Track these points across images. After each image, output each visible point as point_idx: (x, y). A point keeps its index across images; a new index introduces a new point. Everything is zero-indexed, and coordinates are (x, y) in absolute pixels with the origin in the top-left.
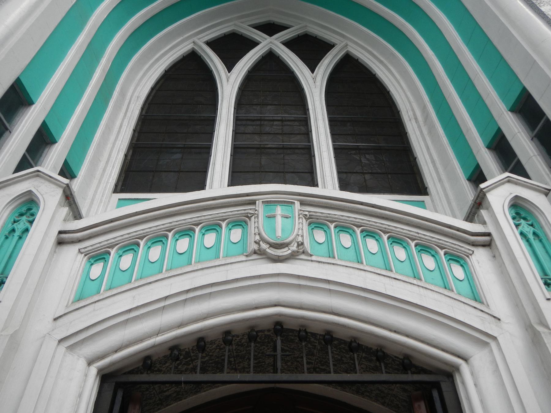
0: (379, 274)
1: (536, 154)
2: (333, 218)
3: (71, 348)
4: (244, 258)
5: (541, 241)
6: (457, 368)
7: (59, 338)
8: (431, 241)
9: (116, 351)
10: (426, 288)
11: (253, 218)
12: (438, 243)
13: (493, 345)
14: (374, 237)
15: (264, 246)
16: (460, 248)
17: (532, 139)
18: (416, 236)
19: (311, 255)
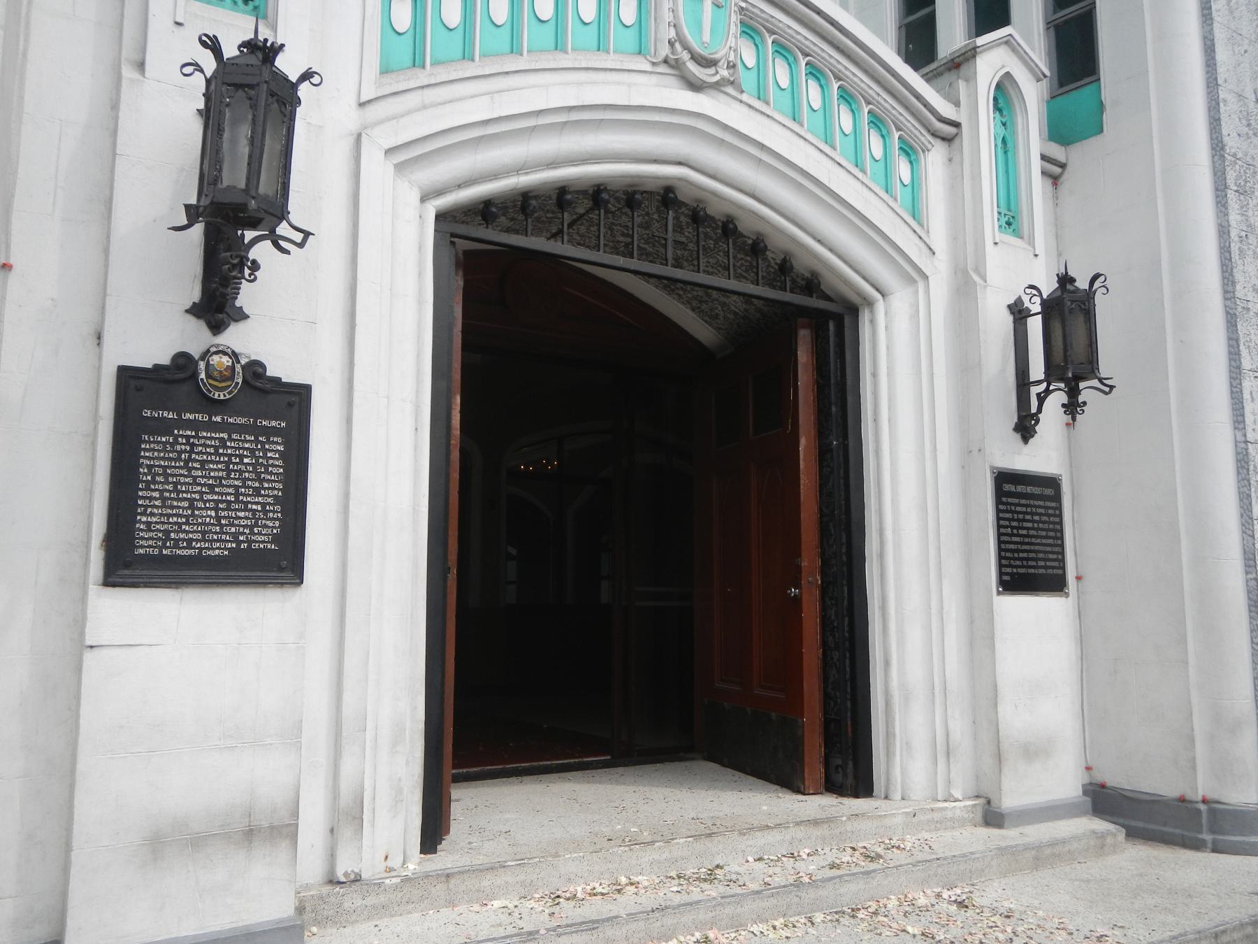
0: (821, 151)
2: (775, 26)
3: (400, 167)
4: (648, 67)
5: (1006, 152)
6: (870, 304)
8: (890, 112)
9: (459, 186)
10: (870, 189)
12: (897, 119)
13: (921, 285)
14: (818, 79)
16: (920, 136)
18: (873, 99)
19: (742, 92)
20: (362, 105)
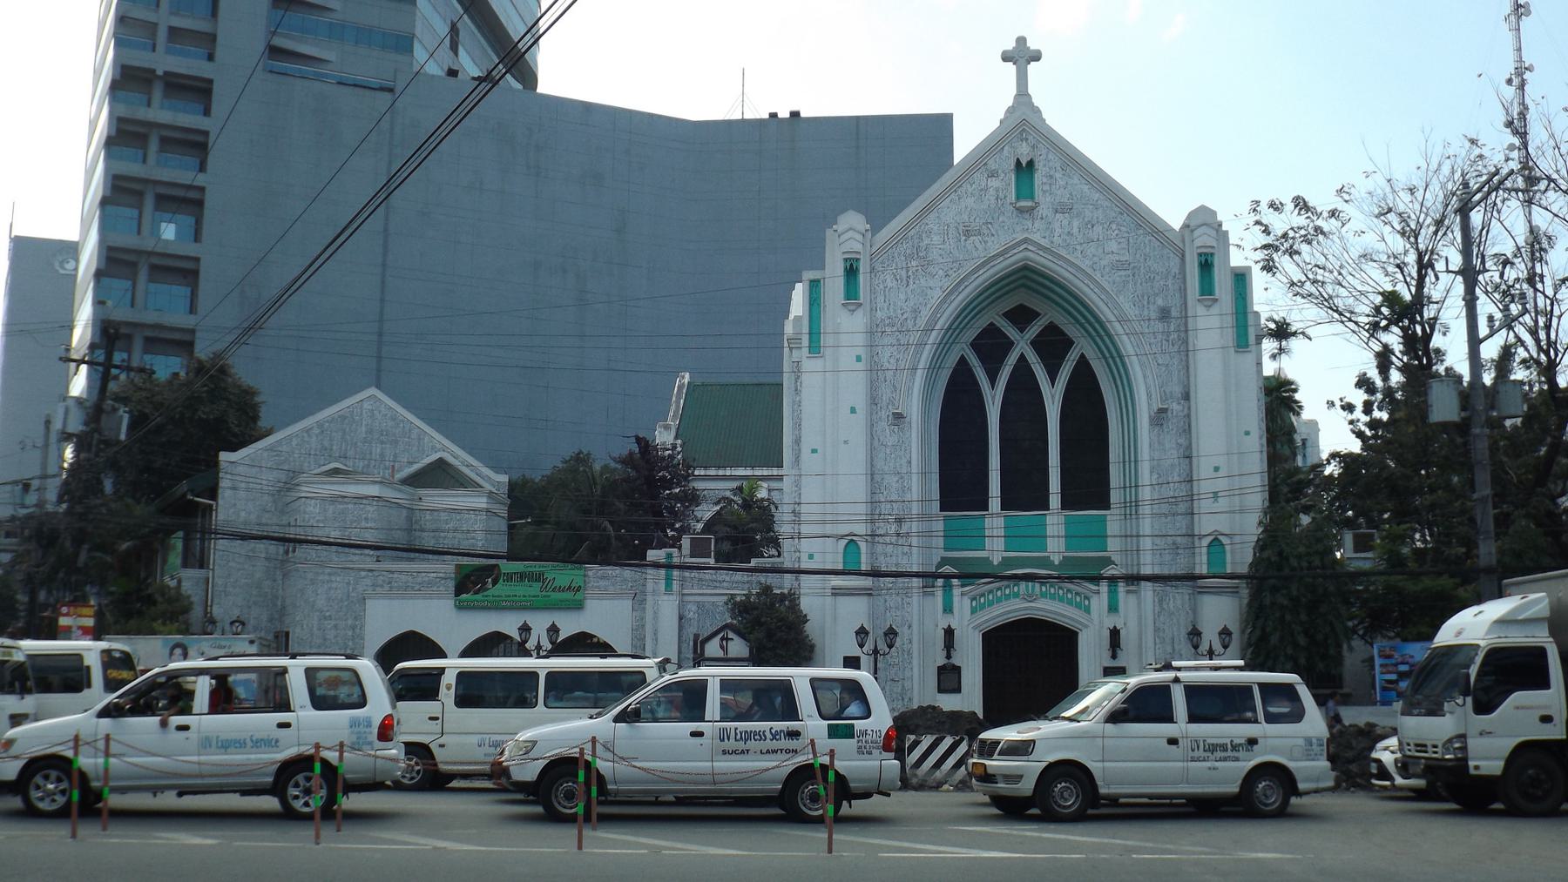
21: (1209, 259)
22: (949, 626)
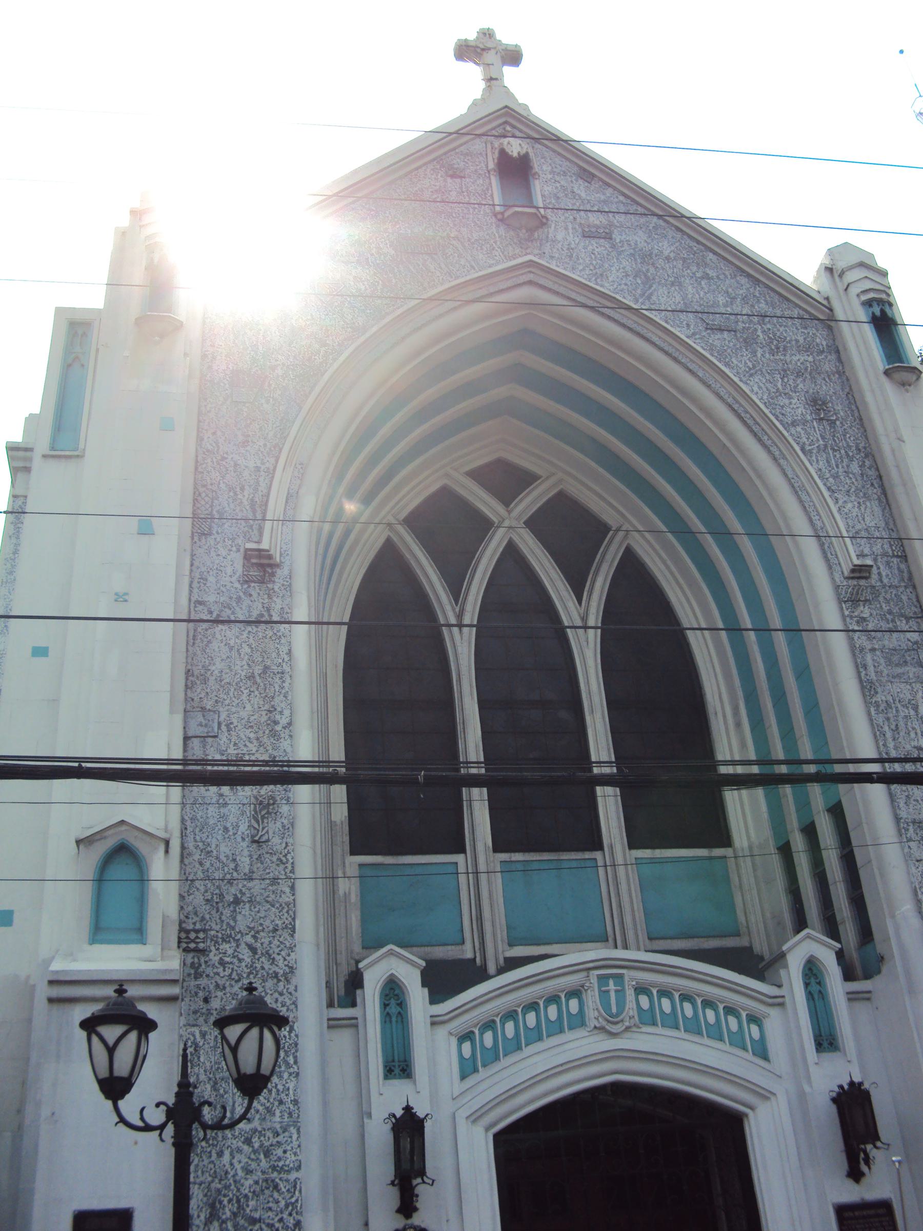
1: (841, 879)
3: (474, 1121)
4: (587, 1034)
6: (746, 1115)
7: (466, 1116)
11: (589, 991)
13: (773, 1098)
15: (604, 1023)
17: (841, 858)
20: (453, 1099)
21: (887, 310)
22: (408, 1109)
